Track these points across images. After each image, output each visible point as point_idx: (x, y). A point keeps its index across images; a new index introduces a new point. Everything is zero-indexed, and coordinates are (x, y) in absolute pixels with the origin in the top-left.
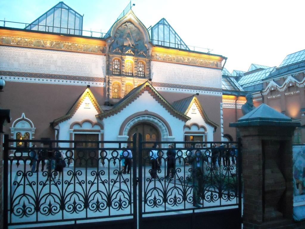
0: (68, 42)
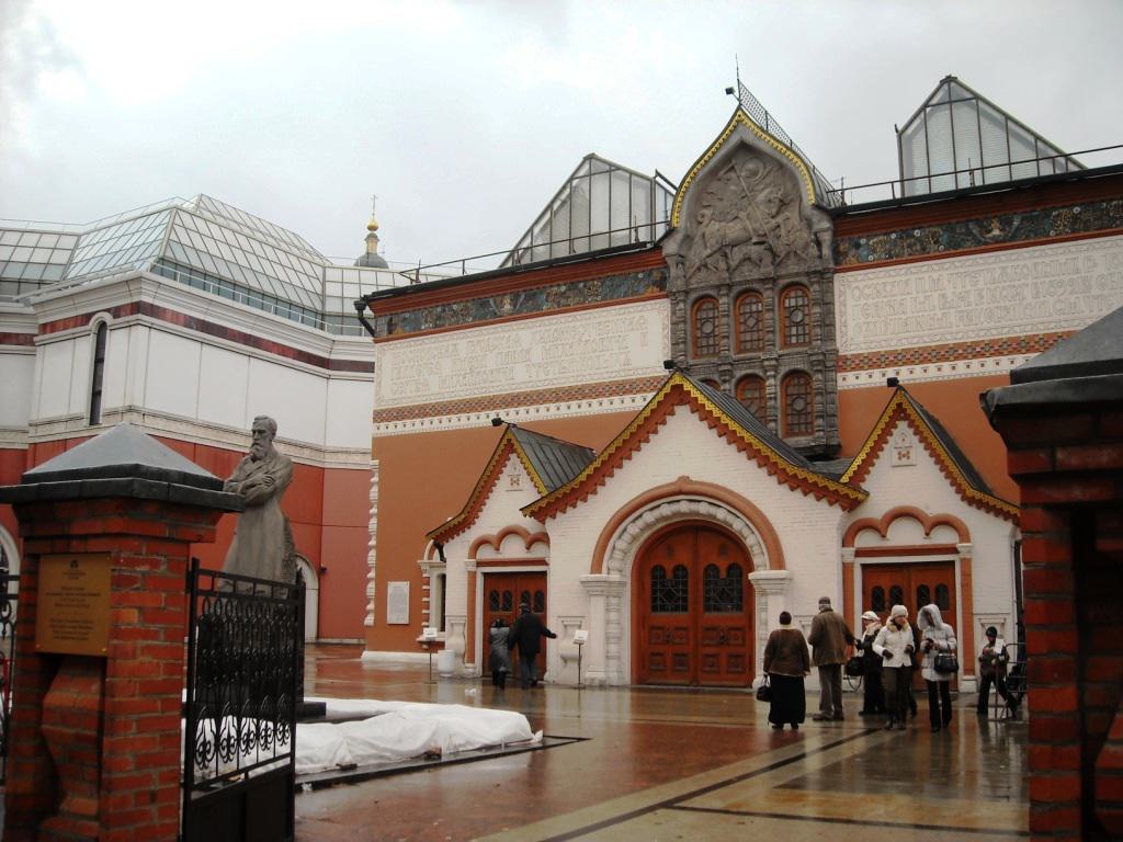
0: (561, 283)
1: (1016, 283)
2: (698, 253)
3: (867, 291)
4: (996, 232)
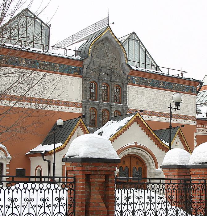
3: (134, 92)
4: (162, 85)
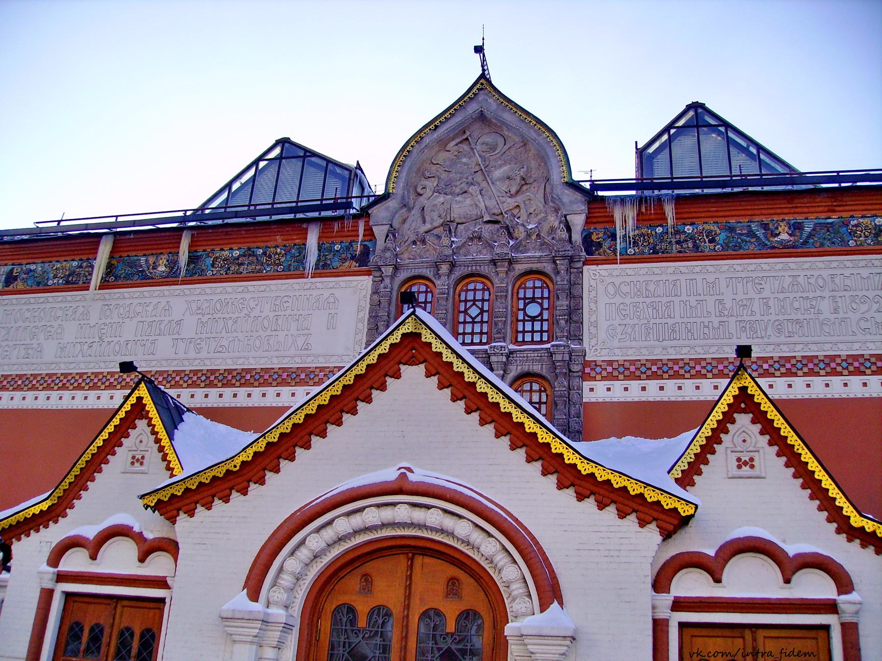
1: (811, 295)
2: (413, 226)
3: (625, 289)
